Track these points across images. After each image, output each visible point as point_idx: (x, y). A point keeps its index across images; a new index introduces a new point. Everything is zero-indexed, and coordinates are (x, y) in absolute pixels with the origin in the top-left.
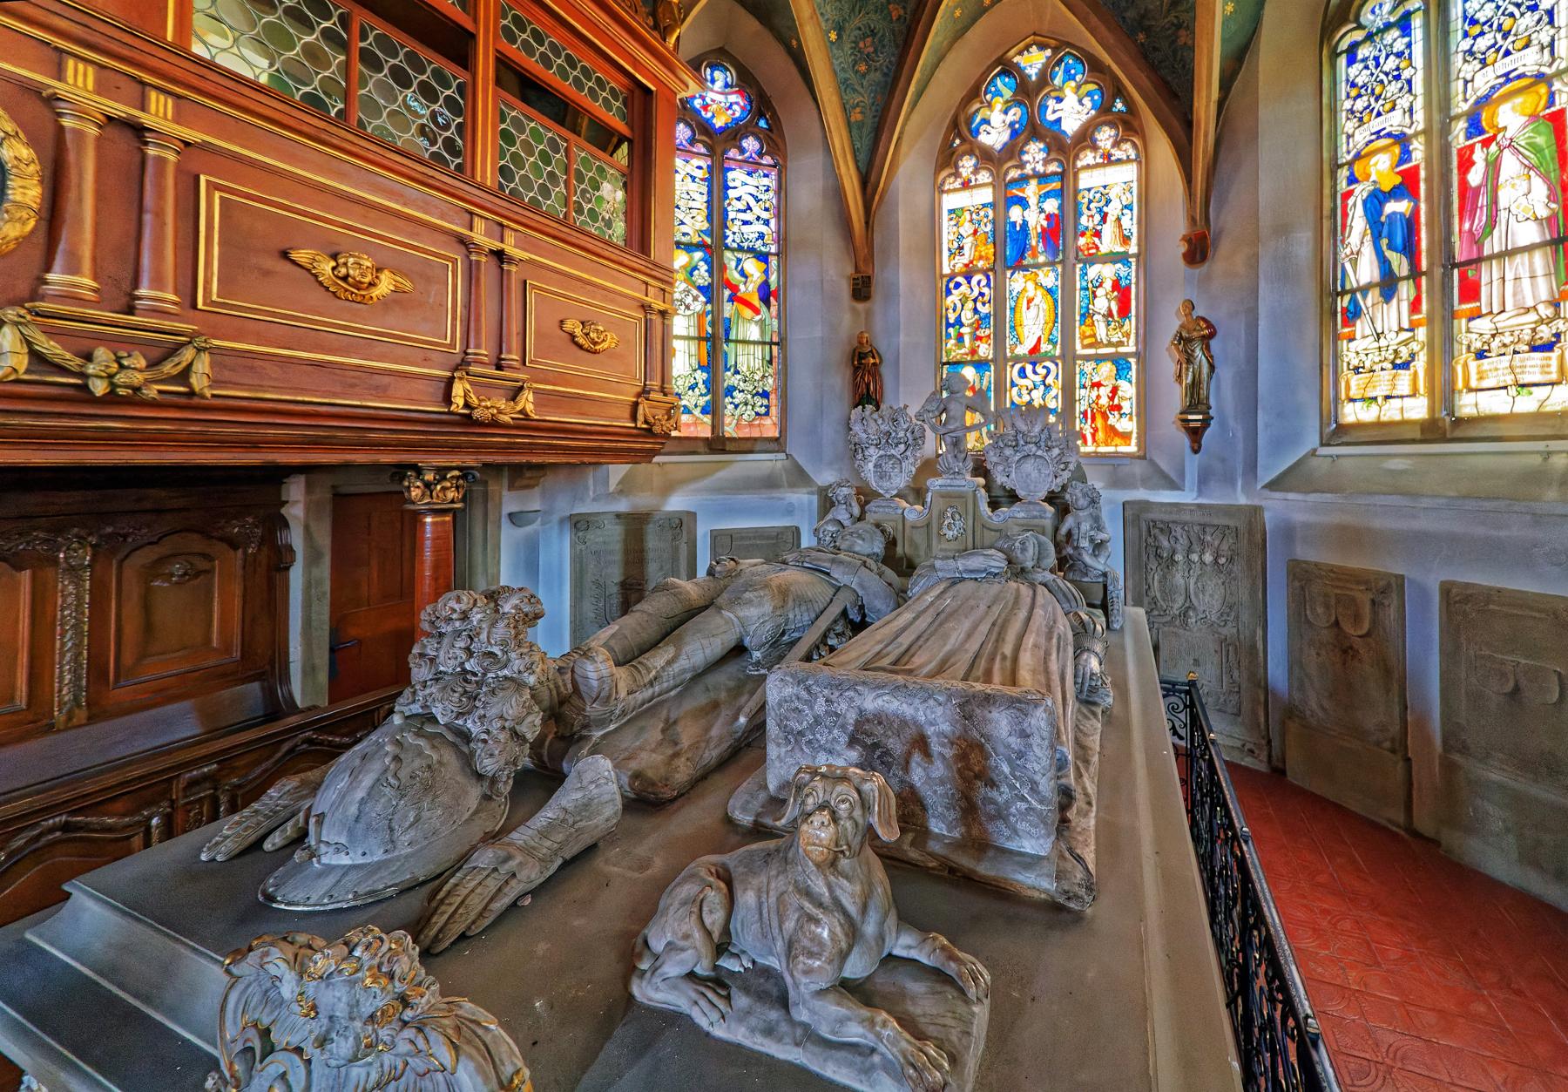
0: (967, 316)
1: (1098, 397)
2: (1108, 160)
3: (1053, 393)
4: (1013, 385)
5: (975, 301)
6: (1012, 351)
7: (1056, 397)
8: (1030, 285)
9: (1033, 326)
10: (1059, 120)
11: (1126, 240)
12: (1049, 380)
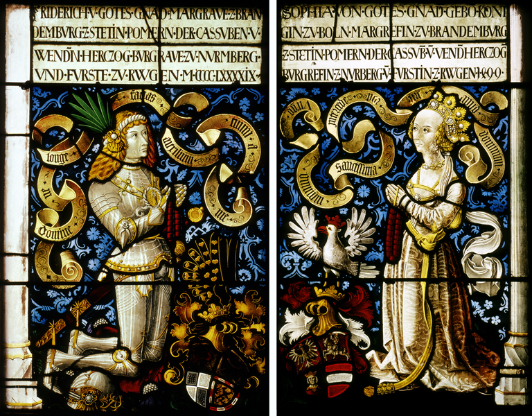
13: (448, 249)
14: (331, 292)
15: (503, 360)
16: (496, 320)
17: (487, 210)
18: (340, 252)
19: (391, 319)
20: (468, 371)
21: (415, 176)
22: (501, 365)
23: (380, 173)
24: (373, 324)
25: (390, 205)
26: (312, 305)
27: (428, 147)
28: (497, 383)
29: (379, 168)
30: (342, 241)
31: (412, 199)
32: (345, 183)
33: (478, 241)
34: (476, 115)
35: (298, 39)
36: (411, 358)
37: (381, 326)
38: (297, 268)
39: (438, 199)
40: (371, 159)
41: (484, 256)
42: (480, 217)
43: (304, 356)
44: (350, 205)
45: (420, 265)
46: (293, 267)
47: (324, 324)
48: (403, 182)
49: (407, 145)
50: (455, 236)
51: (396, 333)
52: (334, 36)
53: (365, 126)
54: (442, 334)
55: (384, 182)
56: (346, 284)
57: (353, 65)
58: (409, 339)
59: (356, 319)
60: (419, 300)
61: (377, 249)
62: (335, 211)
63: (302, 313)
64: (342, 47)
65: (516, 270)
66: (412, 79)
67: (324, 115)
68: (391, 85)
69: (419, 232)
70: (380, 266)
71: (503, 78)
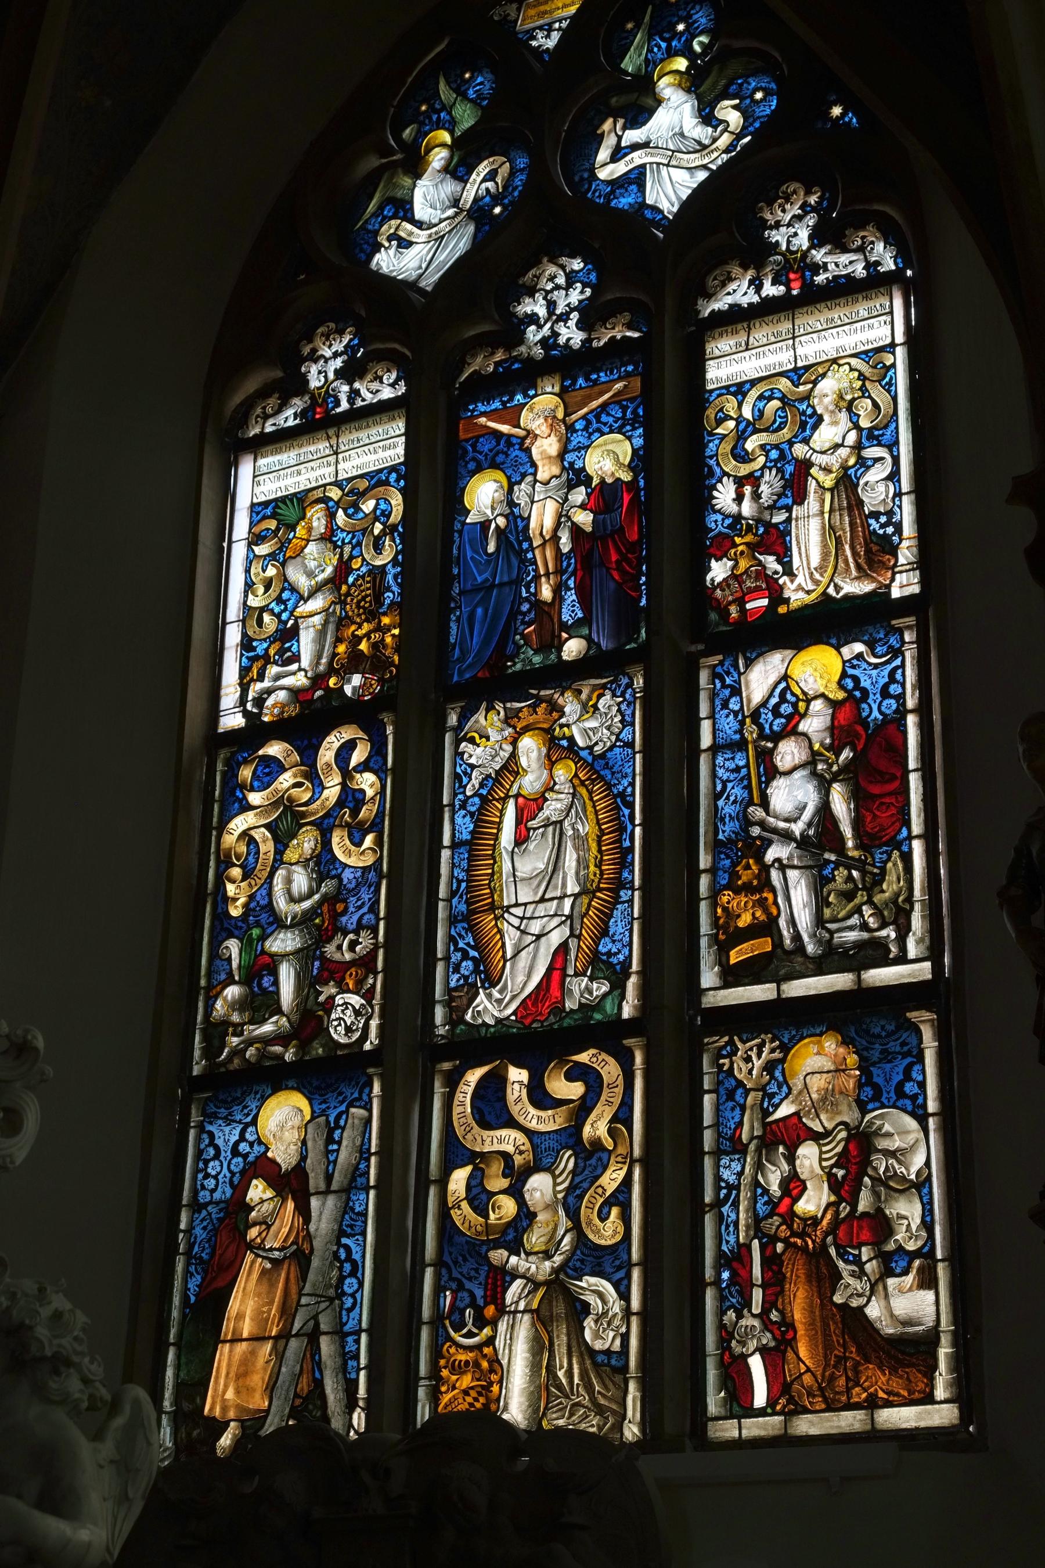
1: (793, 1186)
2: (812, 294)
3: (611, 1179)
4: (456, 1153)
6: (455, 1018)
7: (620, 1198)
8: (530, 747)
9: (539, 904)
10: (637, 178)
11: (877, 552)
12: (597, 1127)
13: (847, 484)
14: (749, 538)
15: (897, 561)
16: (890, 530)
17: (879, 445)
18: (755, 505)
20: (867, 575)
21: (817, 432)
22: (895, 565)
23: (788, 437)
24: (784, 555)
25: (796, 459)
27: (826, 409)
28: (893, 580)
29: (786, 433)
30: (756, 496)
31: (815, 451)
32: (758, 452)
33: (872, 471)
34: (867, 374)
35: (717, 353)
36: (817, 576)
37: (791, 556)
39: (837, 446)
40: (780, 428)
42: (873, 452)
43: (727, 592)
44: (764, 467)
45: (822, 502)
47: (743, 564)
48: (806, 441)
49: (809, 411)
50: (852, 471)
52: (747, 344)
53: (775, 404)
55: (791, 443)
56: (761, 530)
57: (763, 362)
58: (815, 560)
60: (824, 528)
61: (786, 496)
62: (751, 475)
64: (754, 352)
65: (905, 486)
66: (812, 361)
67: (740, 405)
68: (795, 370)
69: (821, 476)
70: (789, 509)
71: (888, 341)
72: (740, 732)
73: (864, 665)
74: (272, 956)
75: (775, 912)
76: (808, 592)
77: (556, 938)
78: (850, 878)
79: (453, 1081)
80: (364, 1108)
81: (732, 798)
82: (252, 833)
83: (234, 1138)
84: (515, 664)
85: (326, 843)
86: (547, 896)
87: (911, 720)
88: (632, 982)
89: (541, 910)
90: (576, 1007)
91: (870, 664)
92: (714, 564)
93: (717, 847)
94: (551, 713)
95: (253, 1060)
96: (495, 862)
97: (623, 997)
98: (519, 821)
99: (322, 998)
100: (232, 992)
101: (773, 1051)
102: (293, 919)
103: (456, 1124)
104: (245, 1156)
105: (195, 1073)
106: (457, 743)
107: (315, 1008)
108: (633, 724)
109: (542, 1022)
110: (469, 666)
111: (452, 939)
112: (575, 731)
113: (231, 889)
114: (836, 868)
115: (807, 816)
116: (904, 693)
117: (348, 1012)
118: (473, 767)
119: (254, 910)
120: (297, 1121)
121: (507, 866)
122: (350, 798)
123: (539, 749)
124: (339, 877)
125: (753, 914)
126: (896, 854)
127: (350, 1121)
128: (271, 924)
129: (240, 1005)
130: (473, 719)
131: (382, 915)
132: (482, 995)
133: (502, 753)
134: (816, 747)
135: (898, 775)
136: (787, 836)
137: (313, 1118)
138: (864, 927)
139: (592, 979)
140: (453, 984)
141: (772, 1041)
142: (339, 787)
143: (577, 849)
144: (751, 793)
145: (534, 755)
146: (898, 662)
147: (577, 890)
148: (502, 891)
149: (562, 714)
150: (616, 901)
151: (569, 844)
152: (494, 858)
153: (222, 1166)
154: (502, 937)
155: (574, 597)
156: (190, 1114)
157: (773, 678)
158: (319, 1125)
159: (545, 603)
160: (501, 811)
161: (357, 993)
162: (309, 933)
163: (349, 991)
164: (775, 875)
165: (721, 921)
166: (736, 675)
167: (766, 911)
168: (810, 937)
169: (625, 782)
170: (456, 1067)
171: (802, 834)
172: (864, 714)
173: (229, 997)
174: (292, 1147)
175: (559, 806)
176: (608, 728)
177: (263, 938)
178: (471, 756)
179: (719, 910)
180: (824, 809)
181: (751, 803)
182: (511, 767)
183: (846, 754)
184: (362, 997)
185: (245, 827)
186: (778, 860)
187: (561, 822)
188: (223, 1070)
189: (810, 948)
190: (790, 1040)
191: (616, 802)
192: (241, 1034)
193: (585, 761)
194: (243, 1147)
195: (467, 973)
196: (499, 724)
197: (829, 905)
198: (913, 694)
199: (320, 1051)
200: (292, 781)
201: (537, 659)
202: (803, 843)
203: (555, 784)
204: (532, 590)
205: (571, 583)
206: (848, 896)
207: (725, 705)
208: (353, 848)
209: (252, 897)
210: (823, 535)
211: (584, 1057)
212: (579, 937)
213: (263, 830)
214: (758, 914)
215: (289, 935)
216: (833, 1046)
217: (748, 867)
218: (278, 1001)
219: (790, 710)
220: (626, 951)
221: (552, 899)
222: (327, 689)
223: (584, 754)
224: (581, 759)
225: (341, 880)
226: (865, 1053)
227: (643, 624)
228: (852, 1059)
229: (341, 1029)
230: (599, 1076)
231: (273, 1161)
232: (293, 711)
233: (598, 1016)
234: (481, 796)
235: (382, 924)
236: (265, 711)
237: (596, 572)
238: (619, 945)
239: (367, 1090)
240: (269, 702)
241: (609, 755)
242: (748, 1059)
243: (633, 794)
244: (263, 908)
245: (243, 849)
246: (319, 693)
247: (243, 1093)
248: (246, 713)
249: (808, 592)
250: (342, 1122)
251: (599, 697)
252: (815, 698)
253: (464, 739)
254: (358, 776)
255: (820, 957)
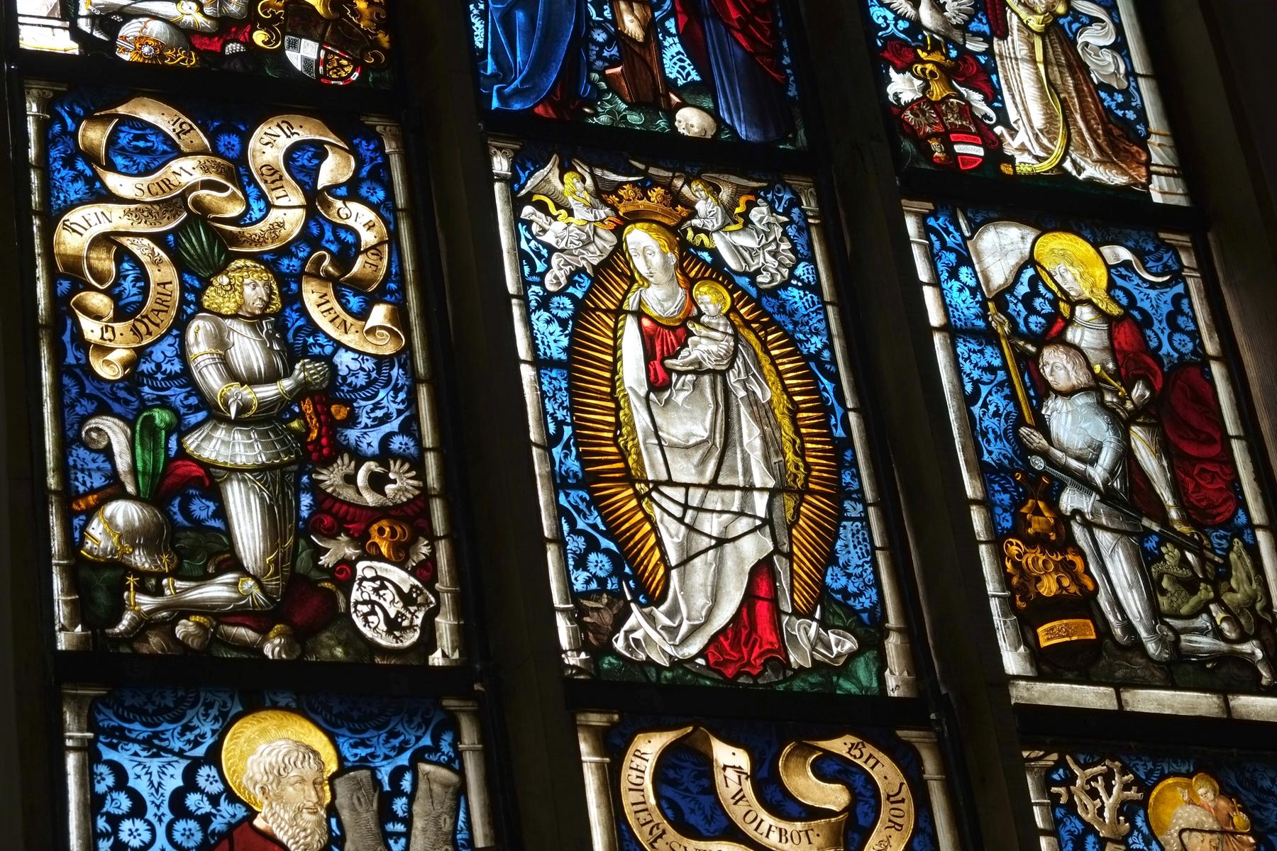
0: (228, 350)
5: (284, 268)
6: (595, 641)
11: (1121, 139)
16: (1131, 115)
19: (1013, 97)
24: (993, 96)
26: (920, 67)
28: (1149, 181)
36: (1045, 141)
37: (1003, 102)
38: (892, 26)
41: (1101, 48)
43: (922, 119)
45: (1032, 47)
46: (888, 25)
47: (937, 91)
51: (1023, 113)
54: (1075, 120)
56: (954, 53)
58: (1039, 121)
59: (975, 90)
63: (908, 74)
72: (984, 316)
73: (1137, 281)
74: (206, 466)
75: (1091, 587)
76: (1037, 158)
77: (752, 548)
78: (1184, 562)
79: (614, 749)
80: (447, 765)
81: (992, 408)
82: (126, 241)
83: (174, 781)
84: (597, 114)
85: (294, 300)
86: (721, 481)
87: (1216, 370)
88: (893, 644)
89: (715, 500)
90: (809, 665)
91: (1145, 281)
92: (892, 72)
93: (983, 471)
94: (674, 205)
95: (194, 643)
96: (619, 408)
97: (882, 664)
98: (649, 356)
99: (326, 560)
100: (124, 512)
101: (1126, 787)
102: (244, 408)
103: (631, 819)
104: (205, 820)
105: (62, 646)
106: (516, 204)
107: (314, 574)
108: (812, 260)
109: (755, 678)
110: (517, 93)
111: (560, 512)
112: (718, 242)
113: (91, 329)
114: (1161, 543)
115: (1106, 458)
116: (1198, 330)
117: (389, 594)
118: (551, 250)
119: (151, 376)
120: (310, 770)
121: (641, 419)
122: (329, 235)
123: (664, 254)
124: (329, 359)
125: (1059, 581)
126: (1237, 543)
127: (422, 786)
128: (196, 409)
129: (149, 538)
130: (539, 175)
131: (428, 441)
132: (636, 618)
133: (597, 239)
134: (1097, 369)
135: (1217, 437)
136: (1085, 483)
137: (342, 770)
138: (1218, 633)
139: (824, 624)
140: (579, 586)
141: (1123, 772)
142: (301, 213)
143: (758, 421)
144: (1018, 405)
145: (656, 260)
146: (1179, 289)
147: (771, 483)
148: (639, 454)
149: (694, 214)
150: (840, 516)
151: (743, 409)
152: (616, 401)
153: (152, 830)
154: (655, 529)
155: (679, 48)
156: (61, 721)
157: (1013, 260)
158: (358, 784)
159: (633, 40)
160: (615, 330)
161: (401, 565)
162: (282, 442)
163: (380, 558)
164: (1078, 531)
165: (1015, 580)
166: (959, 238)
167: (1075, 579)
168: (1147, 631)
169: (816, 342)
170: (614, 725)
171: (1105, 483)
172: (1153, 344)
173: (120, 521)
174: (306, 816)
175: (714, 348)
176: (775, 254)
177: (180, 429)
178: (544, 231)
179: (1009, 565)
180: (1126, 456)
181: (1020, 421)
182: (616, 266)
183: (1138, 391)
184: (412, 573)
185: (106, 227)
186: (1077, 512)
187: (723, 374)
188: (125, 650)
189: (1151, 647)
190: (1149, 774)
191: (807, 366)
192: (158, 591)
193: (745, 293)
194: (193, 800)
195: (602, 574)
196: (585, 194)
197: (1164, 592)
198: (1211, 338)
199: (339, 652)
200: (199, 176)
201: (635, 119)
202: (1107, 496)
203: (701, 314)
204: (607, 14)
205: (671, 24)
206: (1190, 586)
207: (954, 275)
208: (350, 320)
209: (141, 353)
210: (1042, 88)
211: (839, 745)
212: (790, 556)
213: (146, 241)
214: (1066, 582)
215: (238, 436)
216: (1210, 796)
217: (1037, 512)
218: (231, 546)
219: (1048, 309)
220: (872, 593)
221: (732, 488)
222: (250, 43)
223: (743, 281)
224: (737, 287)
225: (334, 368)
226: (1257, 814)
227: (799, 122)
228: (1240, 819)
229: (378, 620)
230: (870, 780)
231: (269, 837)
232: (178, 58)
233: (848, 686)
234: (572, 297)
235: (431, 459)
236: (120, 42)
237: (710, 25)
238: (859, 583)
239: (447, 738)
240: (130, 30)
241: (782, 294)
242: (1093, 794)
243: (833, 361)
244: (171, 377)
245: (105, 262)
246: (232, 48)
247: (179, 702)
248: (76, 34)
249: (1037, 158)
250: (406, 784)
251: (751, 205)
252: (1082, 302)
253: (528, 199)
254: (339, 204)
255: (1168, 663)
